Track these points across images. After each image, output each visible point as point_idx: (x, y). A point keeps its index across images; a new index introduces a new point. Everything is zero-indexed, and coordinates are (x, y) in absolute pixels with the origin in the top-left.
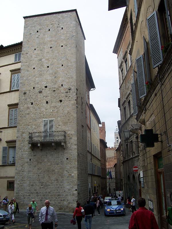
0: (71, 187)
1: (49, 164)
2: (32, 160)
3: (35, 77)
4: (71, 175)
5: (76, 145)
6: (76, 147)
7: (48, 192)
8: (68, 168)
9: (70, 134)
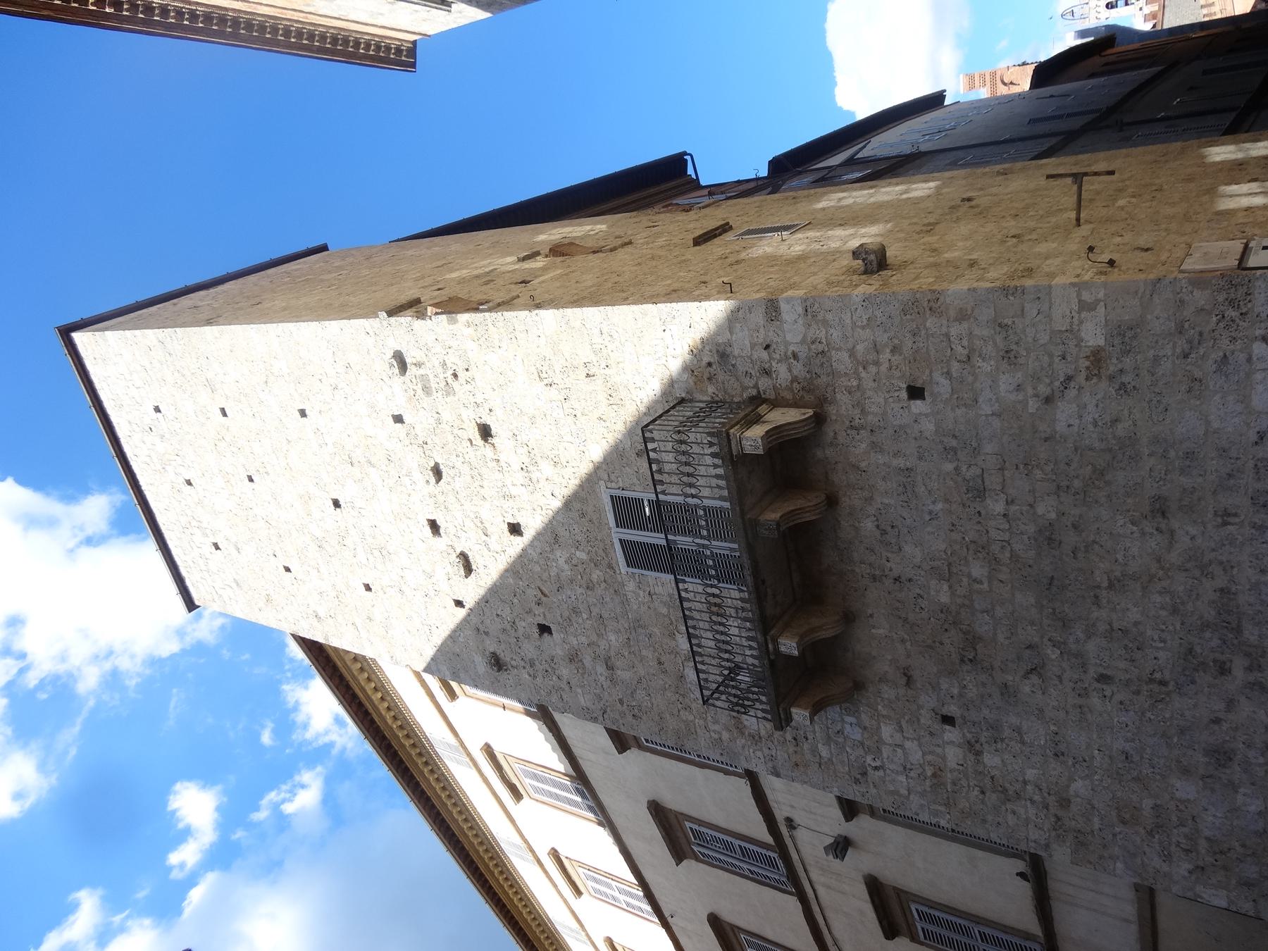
1: (977, 570)
2: (952, 709)
4: (1097, 358)
8: (1019, 388)
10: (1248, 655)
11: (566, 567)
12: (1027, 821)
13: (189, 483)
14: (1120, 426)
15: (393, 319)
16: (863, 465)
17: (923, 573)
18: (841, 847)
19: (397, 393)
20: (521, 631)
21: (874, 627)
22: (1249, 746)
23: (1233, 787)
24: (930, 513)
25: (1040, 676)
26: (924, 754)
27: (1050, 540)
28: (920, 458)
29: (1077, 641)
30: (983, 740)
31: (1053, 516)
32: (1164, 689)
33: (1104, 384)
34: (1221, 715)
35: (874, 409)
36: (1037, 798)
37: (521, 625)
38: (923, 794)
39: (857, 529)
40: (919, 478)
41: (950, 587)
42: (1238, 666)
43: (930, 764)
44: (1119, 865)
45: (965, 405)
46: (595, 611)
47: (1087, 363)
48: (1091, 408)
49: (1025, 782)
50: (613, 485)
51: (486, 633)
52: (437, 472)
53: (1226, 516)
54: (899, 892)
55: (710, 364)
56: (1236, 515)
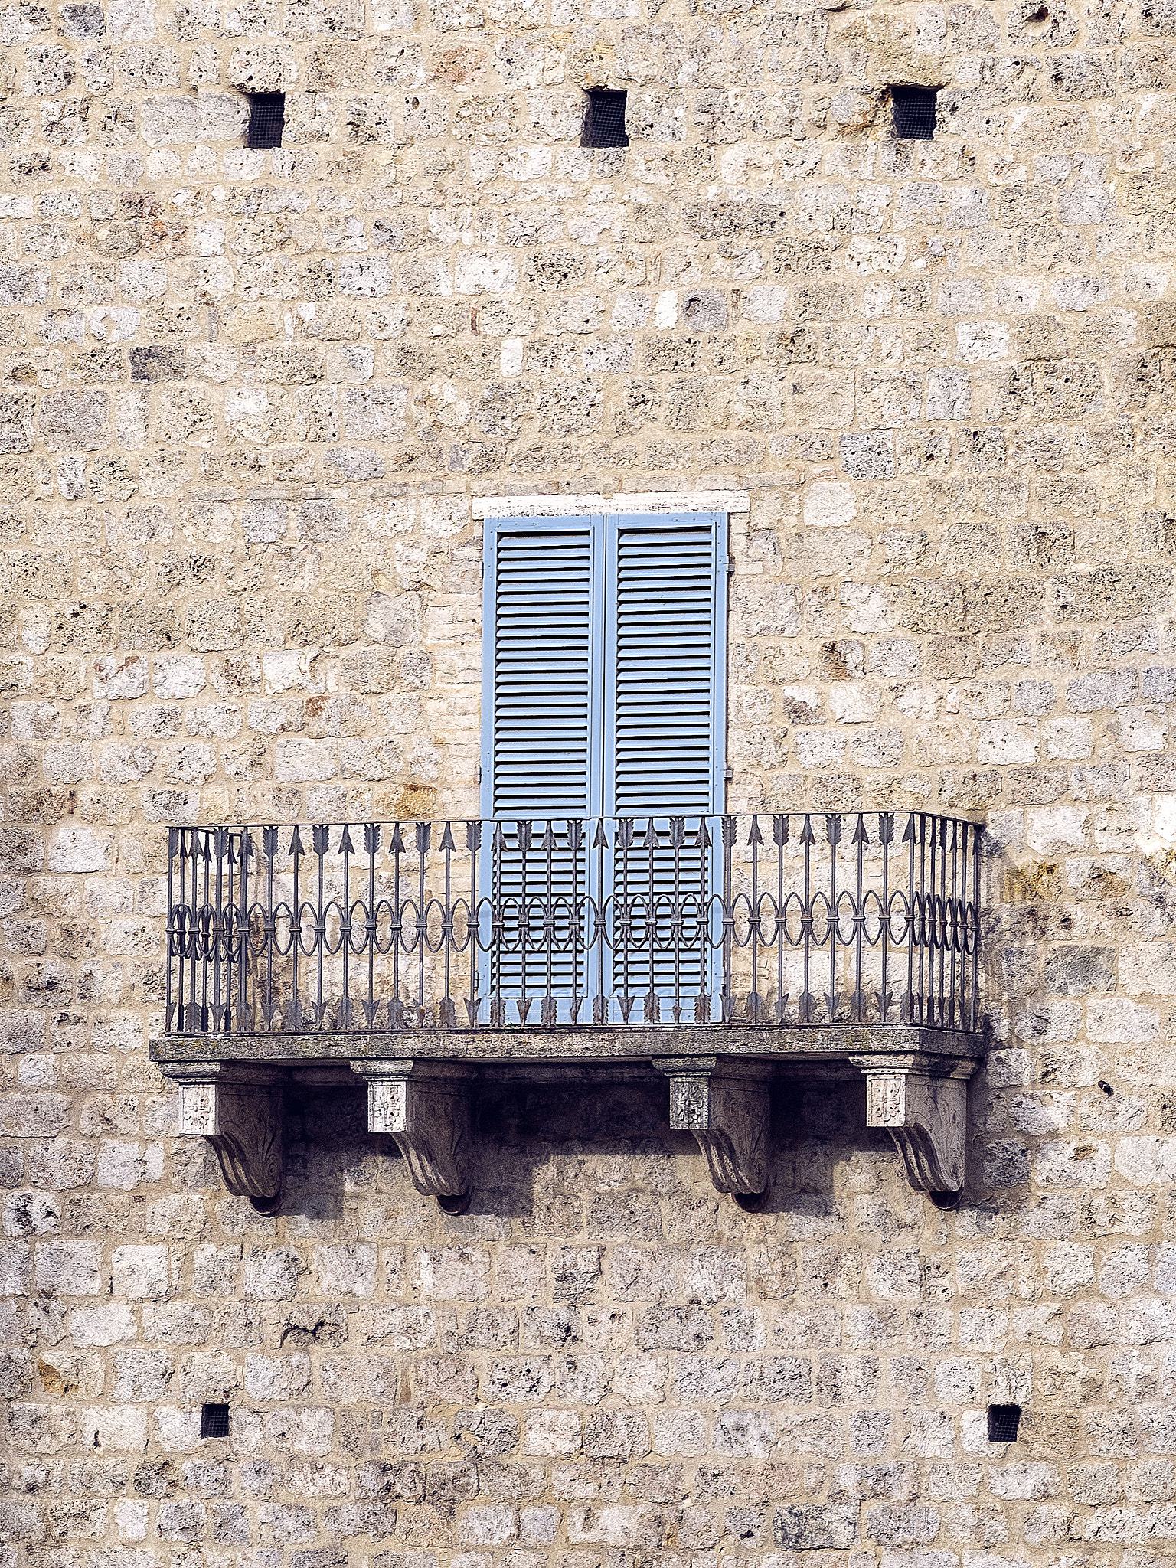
9: (1075, 871)
16: (841, 1284)
17: (594, 1396)
21: (435, 1260)
24: (740, 1429)
28: (863, 1418)
30: (184, 1499)
35: (969, 1328)
39: (683, 1248)
40: (814, 1410)
41: (568, 1457)
45: (980, 1525)
55: (1066, 922)
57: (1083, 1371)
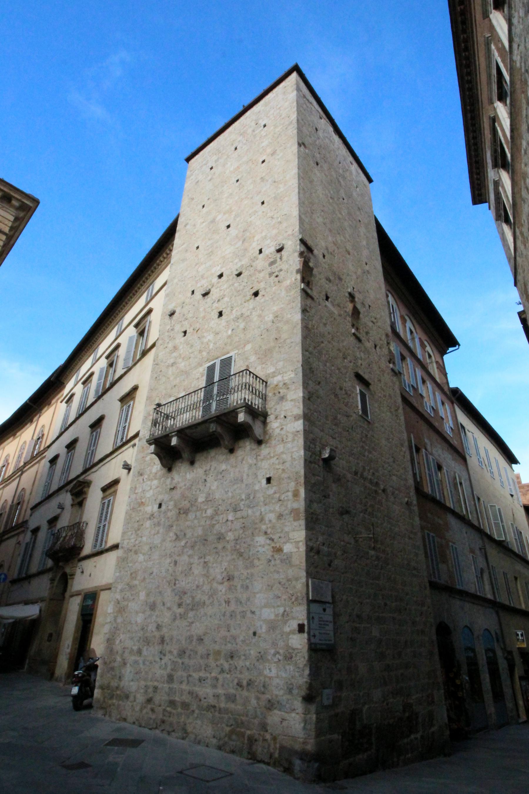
0: (281, 610)
1: (210, 512)
2: (164, 507)
3: (197, 267)
4: (279, 550)
5: (298, 419)
6: (299, 425)
7: (195, 638)
8: (270, 521)
9: (281, 384)
10: (185, 613)
11: (207, 340)
12: (130, 539)
13: (236, 149)
14: (257, 561)
15: (298, 242)
16: (244, 462)
18: (127, 467)
19: (270, 250)
20: (184, 323)
22: (157, 616)
23: (144, 612)
24: (228, 491)
25: (176, 539)
26: (149, 498)
27: (219, 539)
28: (246, 485)
29: (187, 552)
31: (228, 539)
32: (173, 585)
33: (271, 554)
34: (166, 606)
35: (263, 464)
36: (137, 542)
37: (186, 323)
38: (136, 499)
39: (222, 462)
40: (239, 485)
41: (203, 502)
42: (181, 610)
43: (146, 500)
44: (118, 574)
45: (264, 501)
46: (192, 355)
47: (278, 547)
48: (263, 549)
49: (141, 537)
50: (236, 356)
51: (183, 307)
52: (239, 275)
53: (228, 602)
54: (115, 492)
55: (279, 393)
56: (228, 605)
57: (282, 468)
